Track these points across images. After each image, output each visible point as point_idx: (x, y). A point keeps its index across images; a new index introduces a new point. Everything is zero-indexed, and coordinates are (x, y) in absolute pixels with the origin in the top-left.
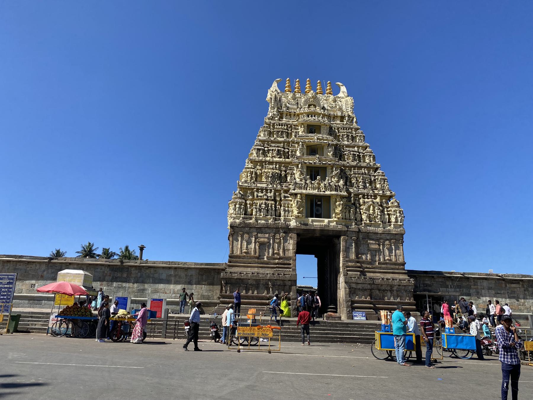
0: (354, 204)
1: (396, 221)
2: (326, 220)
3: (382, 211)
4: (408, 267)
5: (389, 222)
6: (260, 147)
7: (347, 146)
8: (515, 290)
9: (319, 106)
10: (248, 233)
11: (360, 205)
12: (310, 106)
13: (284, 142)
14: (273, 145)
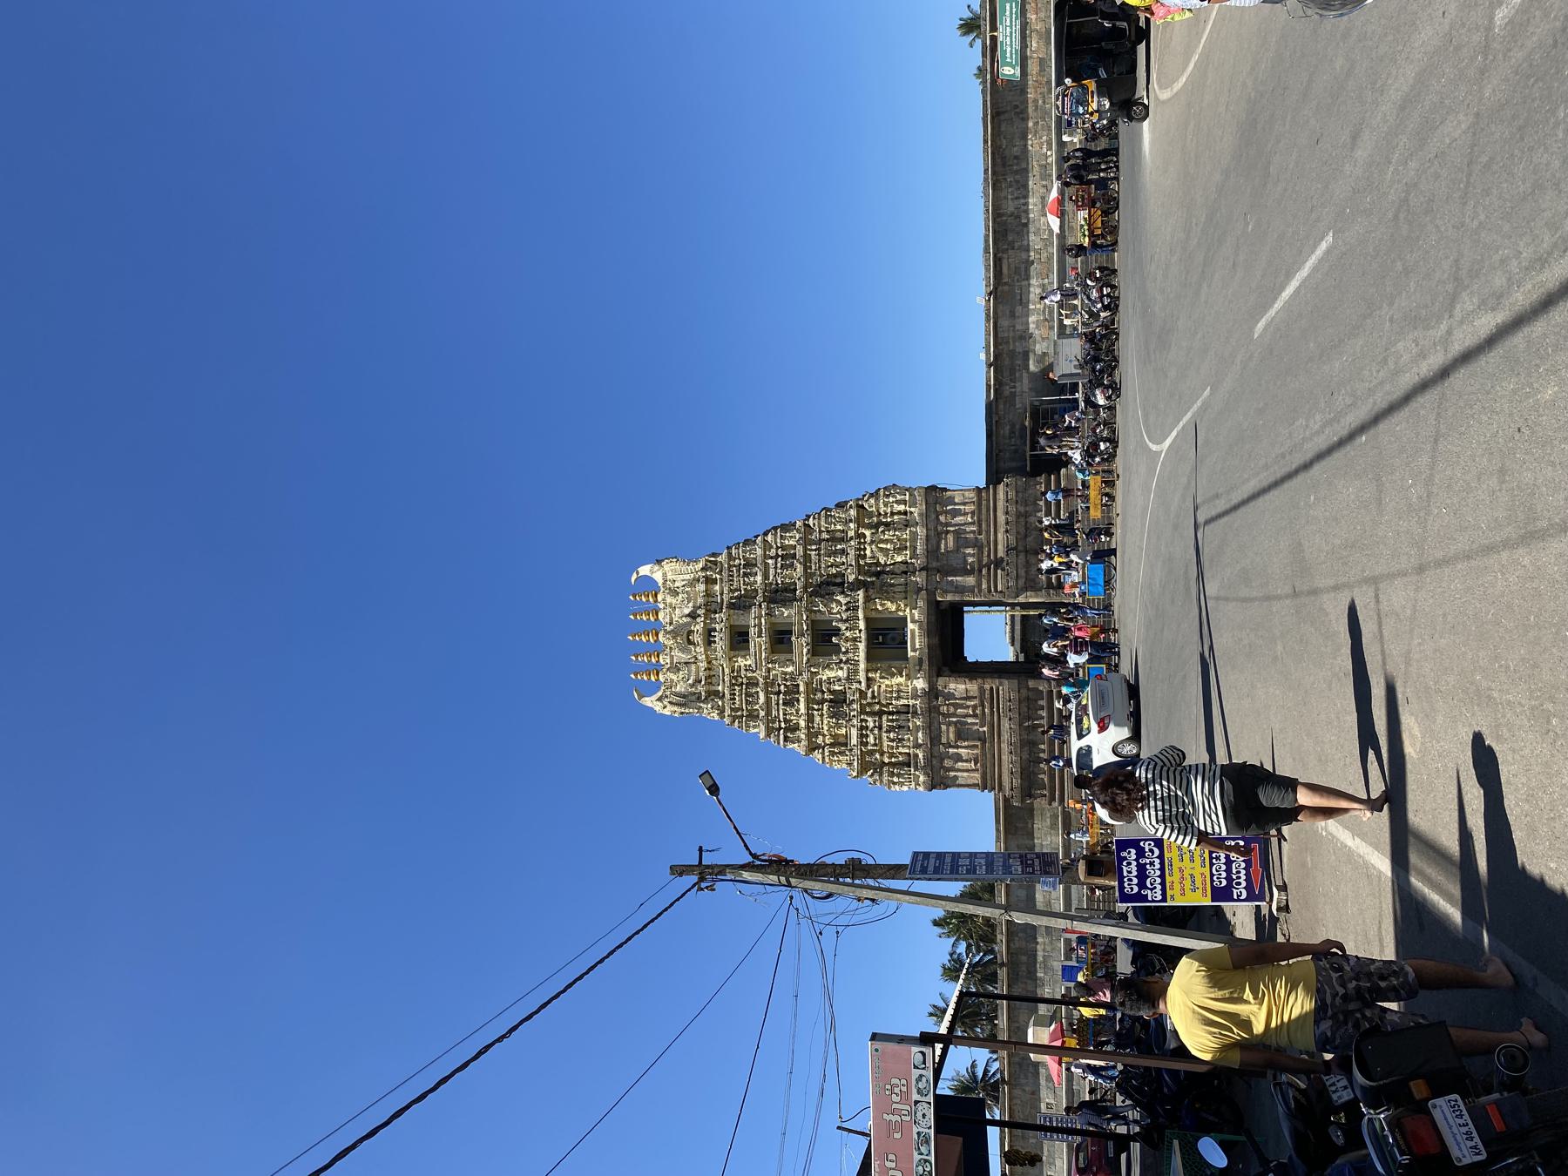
0: (878, 574)
1: (904, 502)
2: (910, 626)
3: (887, 525)
4: (982, 484)
5: (905, 513)
7: (766, 576)
9: (689, 624)
10: (942, 760)
11: (878, 564)
12: (690, 642)
13: (767, 693)
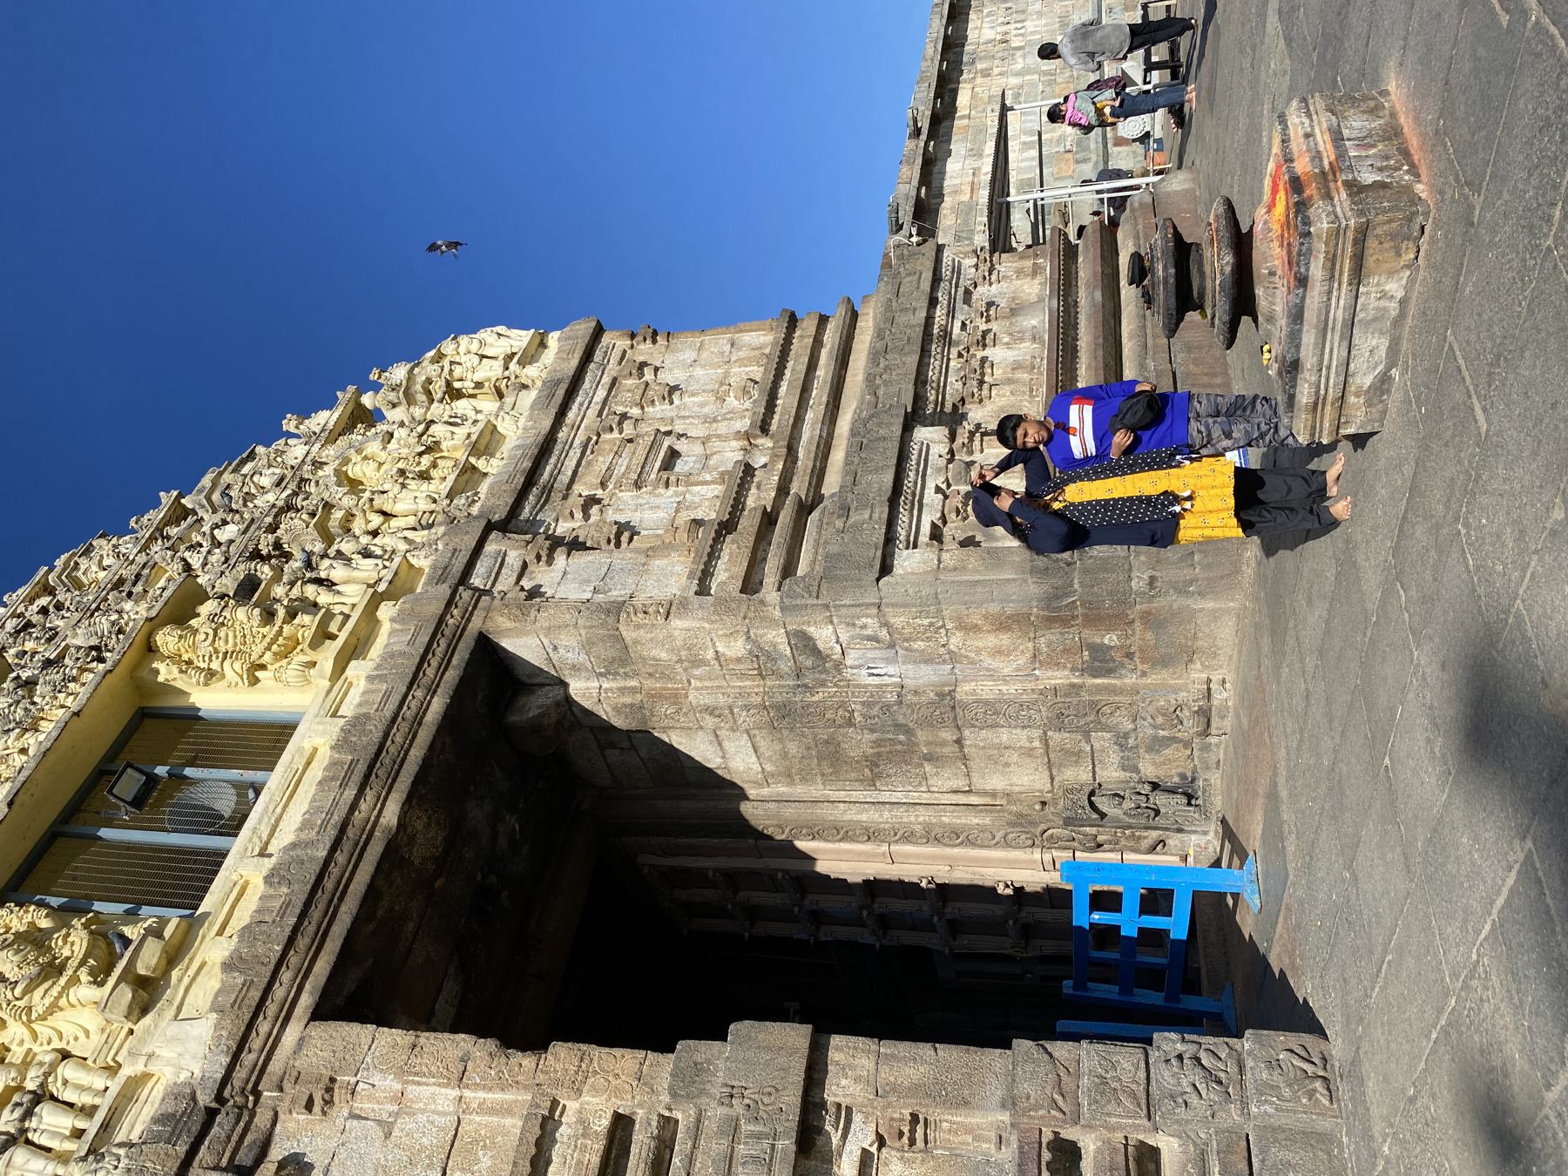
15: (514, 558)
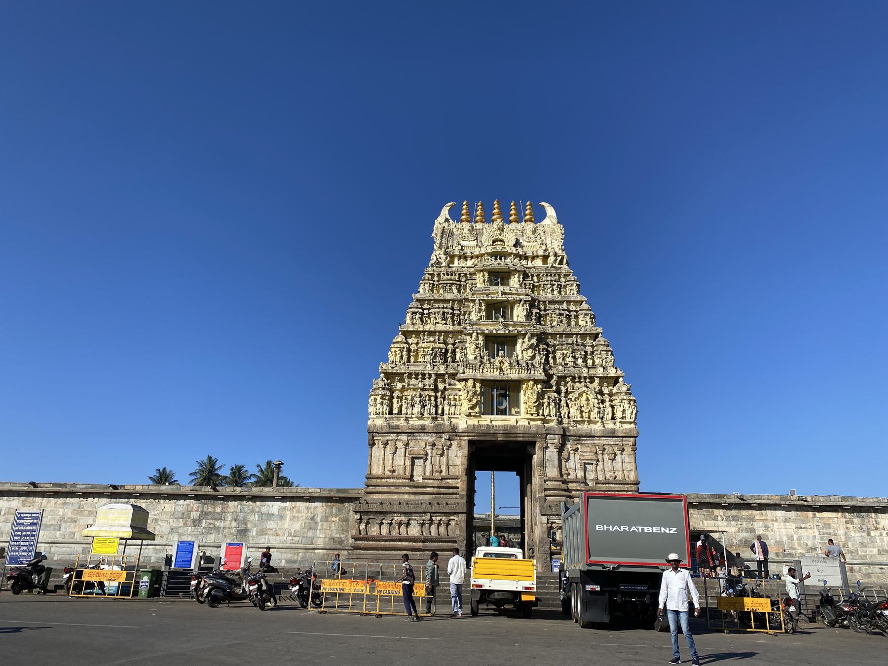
6: (416, 310)
7: (551, 302)
8: (830, 522)
14: (437, 305)
15: (556, 441)
